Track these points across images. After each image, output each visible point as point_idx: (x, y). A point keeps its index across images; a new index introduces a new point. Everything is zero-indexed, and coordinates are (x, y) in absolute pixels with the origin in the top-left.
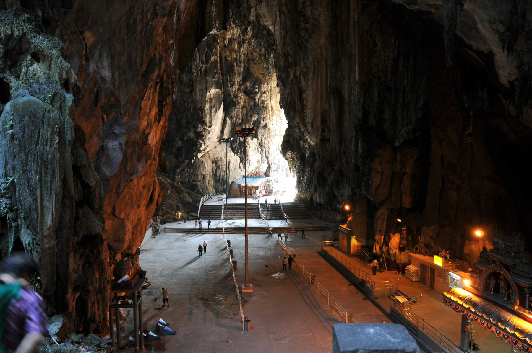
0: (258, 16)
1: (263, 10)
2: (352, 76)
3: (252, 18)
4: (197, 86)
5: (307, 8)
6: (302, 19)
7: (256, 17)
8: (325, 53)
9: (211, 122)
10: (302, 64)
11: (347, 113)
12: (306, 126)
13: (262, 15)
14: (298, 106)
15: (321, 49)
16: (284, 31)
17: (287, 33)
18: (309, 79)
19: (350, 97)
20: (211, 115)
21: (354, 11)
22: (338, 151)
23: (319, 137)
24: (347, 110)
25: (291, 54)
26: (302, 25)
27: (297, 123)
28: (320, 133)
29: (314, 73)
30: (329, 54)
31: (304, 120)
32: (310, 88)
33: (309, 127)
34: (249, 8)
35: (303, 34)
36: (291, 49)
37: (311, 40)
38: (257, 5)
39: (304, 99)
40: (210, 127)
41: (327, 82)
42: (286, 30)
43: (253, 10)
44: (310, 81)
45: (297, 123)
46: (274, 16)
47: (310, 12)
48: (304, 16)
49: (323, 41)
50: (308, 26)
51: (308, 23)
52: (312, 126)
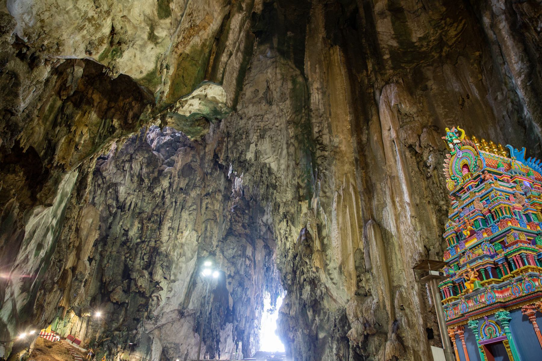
0: (257, 155)
1: (266, 146)
2: (397, 199)
3: (250, 156)
4: (166, 223)
5: (324, 137)
6: (318, 146)
7: (256, 153)
8: (352, 180)
9: (175, 275)
10: (321, 193)
11: (397, 248)
12: (329, 274)
13: (263, 152)
14: (317, 245)
15: (346, 176)
16: (294, 162)
17: (297, 164)
18: (331, 212)
19: (398, 228)
20: (177, 264)
21: (389, 130)
22: (388, 308)
23: (354, 289)
24: (396, 244)
25: (303, 185)
26: (318, 153)
27: (317, 268)
28: (354, 281)
29: (339, 202)
30: (359, 181)
31: (327, 265)
32: (334, 221)
33: (335, 275)
34: (248, 145)
35: (319, 162)
36: (303, 181)
37: (333, 168)
38: (258, 141)
39: (324, 238)
40: (174, 281)
41: (358, 213)
42: (295, 161)
43: (253, 146)
44: (334, 213)
45: (317, 268)
46: (280, 150)
47: (328, 140)
48: (321, 144)
49: (347, 167)
50: (326, 153)
51: (326, 151)
52: (341, 272)
